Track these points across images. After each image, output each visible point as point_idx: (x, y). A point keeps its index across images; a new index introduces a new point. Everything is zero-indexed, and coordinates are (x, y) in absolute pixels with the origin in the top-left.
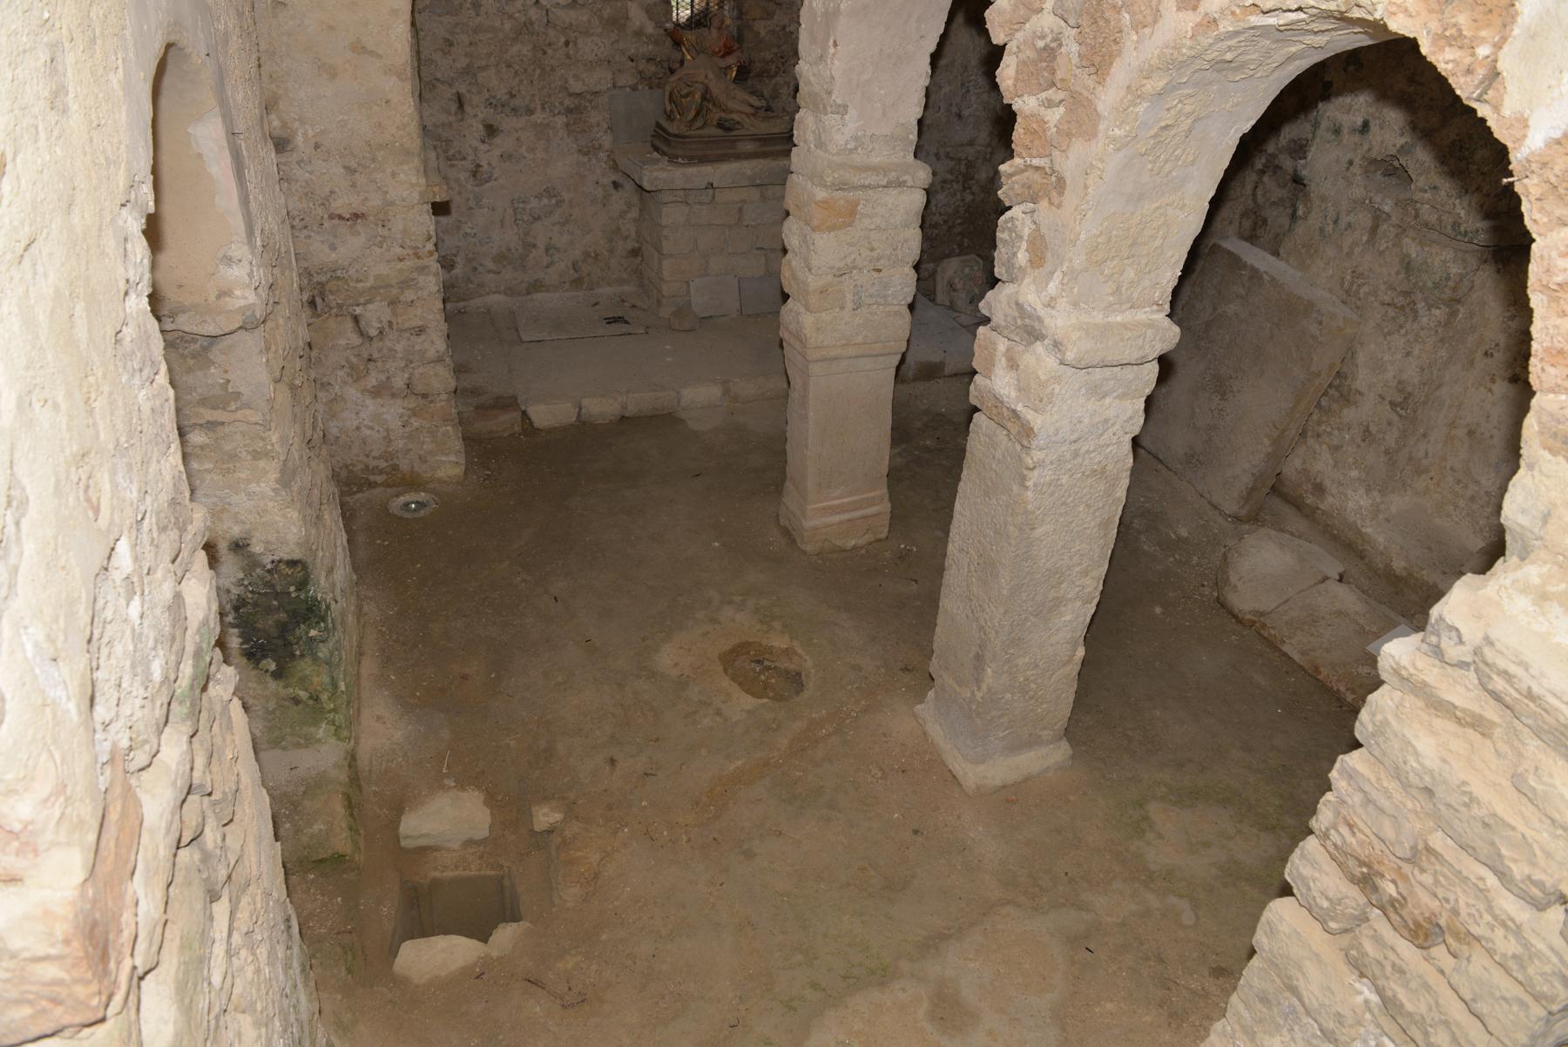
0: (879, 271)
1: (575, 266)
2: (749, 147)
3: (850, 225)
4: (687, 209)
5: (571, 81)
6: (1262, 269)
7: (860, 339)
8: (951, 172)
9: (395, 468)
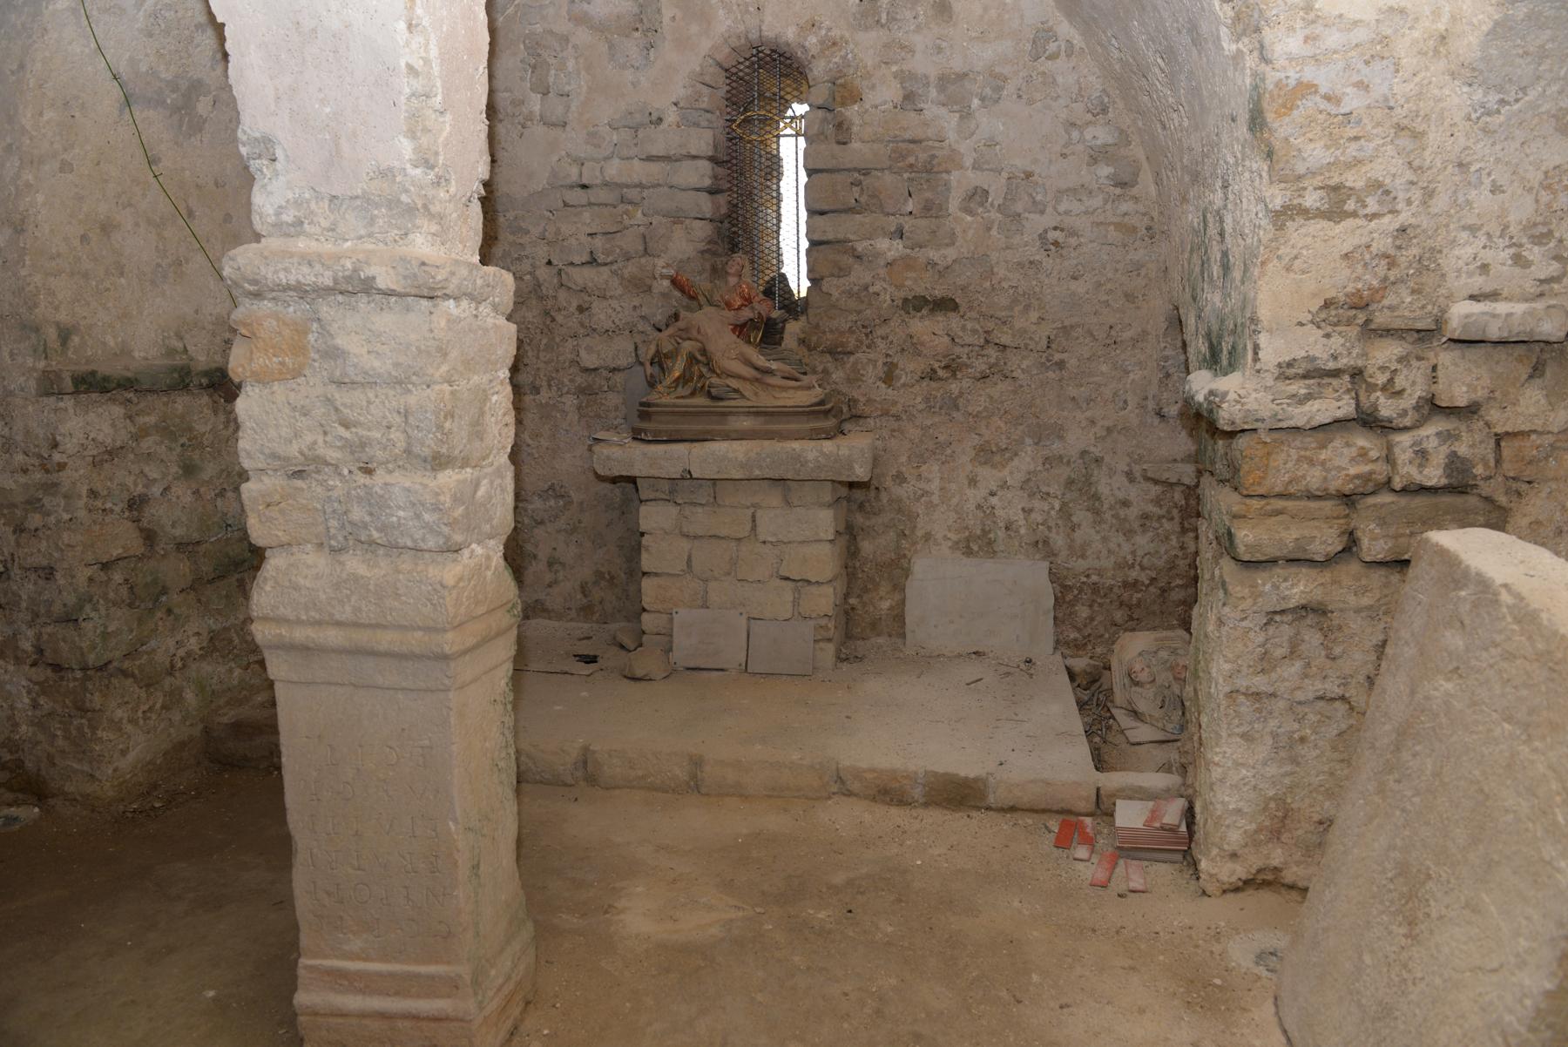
0: (368, 471)
1: (584, 589)
2: (746, 423)
3: (297, 373)
4: (674, 510)
5: (583, 353)
6: (1499, 580)
7: (345, 613)
8: (1157, 502)
9: (20, 764)
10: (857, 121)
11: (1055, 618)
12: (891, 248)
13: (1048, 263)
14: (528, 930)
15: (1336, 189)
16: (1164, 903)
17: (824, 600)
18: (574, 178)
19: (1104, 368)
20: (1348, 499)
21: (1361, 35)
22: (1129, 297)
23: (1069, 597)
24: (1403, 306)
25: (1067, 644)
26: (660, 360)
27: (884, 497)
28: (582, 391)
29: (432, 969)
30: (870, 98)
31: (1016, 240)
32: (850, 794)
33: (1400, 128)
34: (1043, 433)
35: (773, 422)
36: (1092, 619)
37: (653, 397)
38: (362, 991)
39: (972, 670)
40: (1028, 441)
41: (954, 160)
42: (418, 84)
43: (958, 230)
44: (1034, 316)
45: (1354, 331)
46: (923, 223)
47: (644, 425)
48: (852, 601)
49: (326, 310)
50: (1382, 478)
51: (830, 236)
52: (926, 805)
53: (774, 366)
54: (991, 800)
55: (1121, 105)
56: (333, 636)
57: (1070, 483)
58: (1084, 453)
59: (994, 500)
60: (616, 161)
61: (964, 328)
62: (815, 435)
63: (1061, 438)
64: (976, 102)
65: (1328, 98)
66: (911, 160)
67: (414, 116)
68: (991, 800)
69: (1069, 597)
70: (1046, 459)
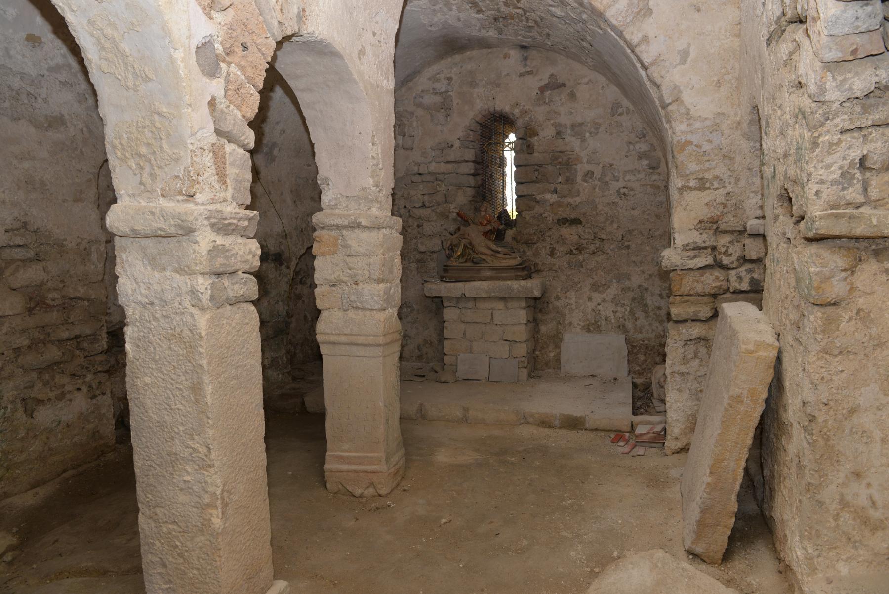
0: (357, 284)
2: (489, 273)
3: (335, 252)
4: (458, 311)
5: (419, 245)
7: (348, 331)
10: (536, 144)
11: (628, 360)
12: (552, 198)
13: (621, 203)
14: (403, 451)
15: (701, 179)
16: (652, 459)
17: (522, 350)
18: (416, 171)
19: (648, 248)
20: (714, 296)
21: (708, 123)
22: (658, 217)
23: (635, 351)
24: (730, 222)
25: (634, 372)
26: (452, 248)
27: (551, 306)
28: (418, 261)
29: (372, 455)
30: (542, 134)
31: (607, 193)
32: (528, 423)
33: (725, 156)
34: (620, 278)
35: (500, 273)
36: (646, 361)
37: (449, 263)
38: (348, 463)
39: (588, 382)
40: (614, 281)
41: (578, 159)
42: (375, 162)
43: (581, 189)
44: (615, 226)
45: (712, 232)
46: (566, 186)
47: (445, 275)
48: (537, 353)
49: (344, 232)
50: (725, 287)
51: (525, 193)
52: (560, 428)
53: (500, 249)
54: (587, 426)
55: (651, 134)
56: (343, 339)
57: (634, 299)
58: (640, 286)
59: (600, 307)
60: (433, 163)
61: (584, 232)
62: (517, 278)
63: (629, 279)
64: (587, 135)
65: (697, 146)
66: (560, 160)
67: (374, 171)
68: (587, 426)
69: (635, 351)
70: (623, 289)
